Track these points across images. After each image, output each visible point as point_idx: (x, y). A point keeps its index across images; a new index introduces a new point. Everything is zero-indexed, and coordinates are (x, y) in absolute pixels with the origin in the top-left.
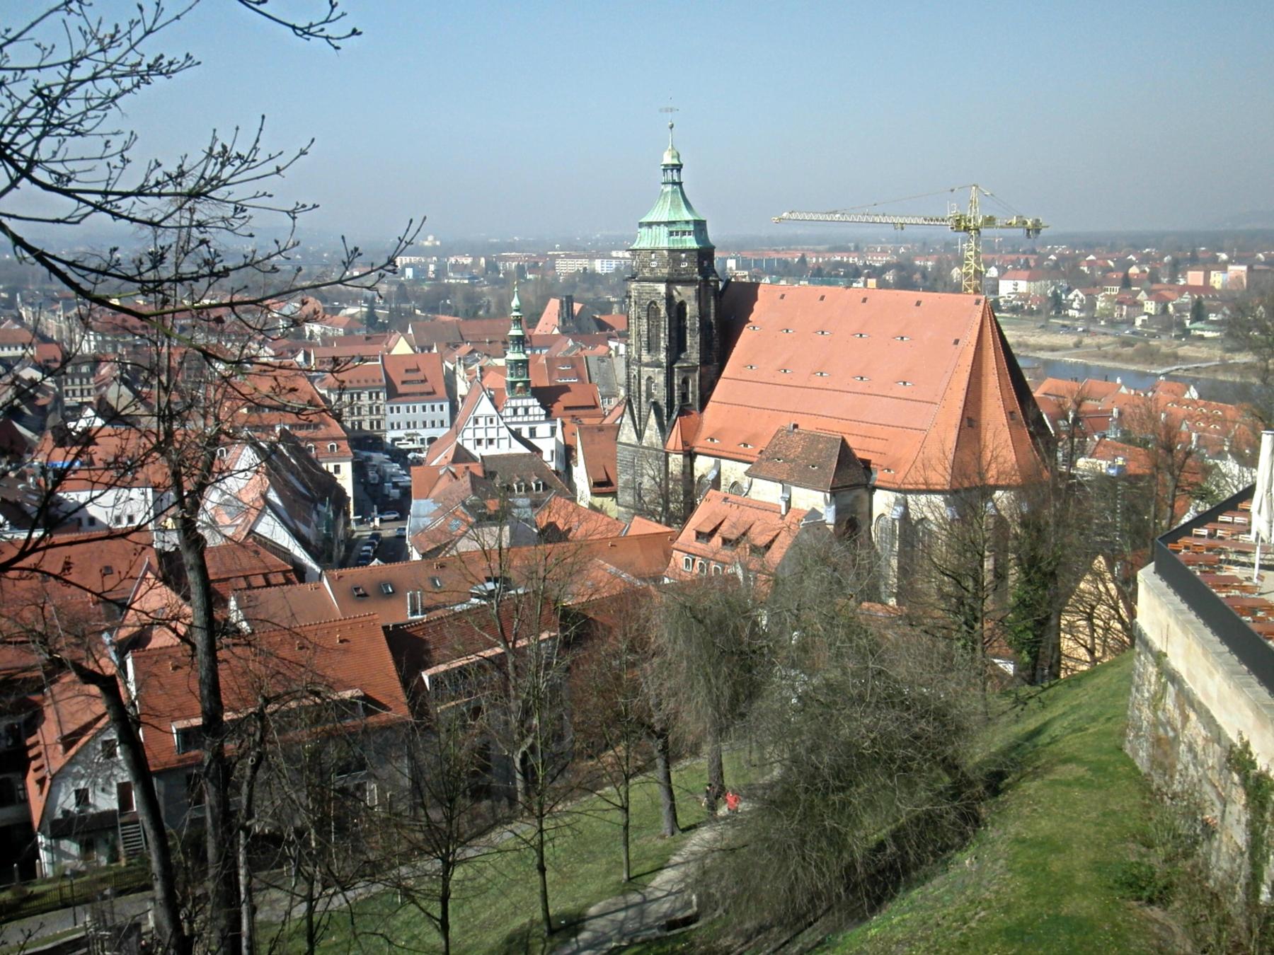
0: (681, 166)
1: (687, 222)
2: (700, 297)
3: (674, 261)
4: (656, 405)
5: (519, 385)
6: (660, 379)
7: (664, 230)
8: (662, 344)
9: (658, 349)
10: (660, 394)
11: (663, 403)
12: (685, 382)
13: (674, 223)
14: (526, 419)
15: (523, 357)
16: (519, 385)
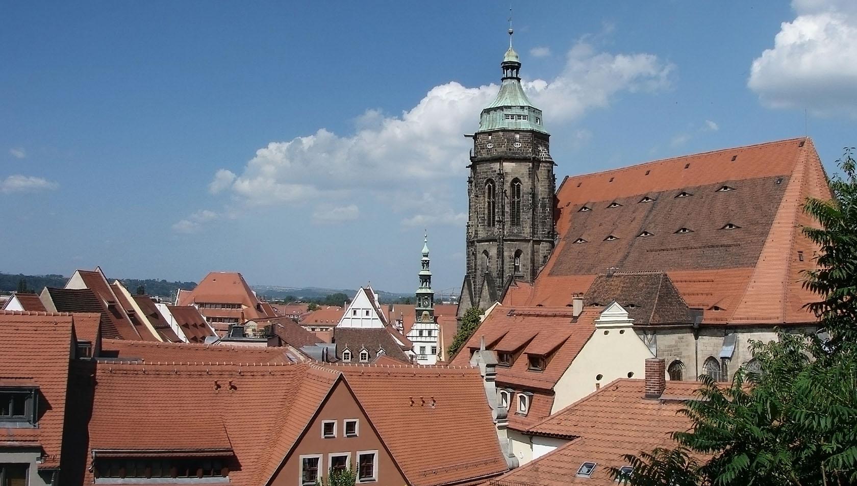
0: (519, 64)
1: (522, 107)
2: (533, 174)
3: (509, 140)
4: (488, 277)
5: (424, 313)
6: (493, 252)
7: (500, 114)
8: (497, 219)
9: (494, 225)
10: (494, 266)
11: (495, 274)
12: (518, 254)
13: (510, 107)
14: (428, 339)
15: (429, 291)
16: (424, 313)
